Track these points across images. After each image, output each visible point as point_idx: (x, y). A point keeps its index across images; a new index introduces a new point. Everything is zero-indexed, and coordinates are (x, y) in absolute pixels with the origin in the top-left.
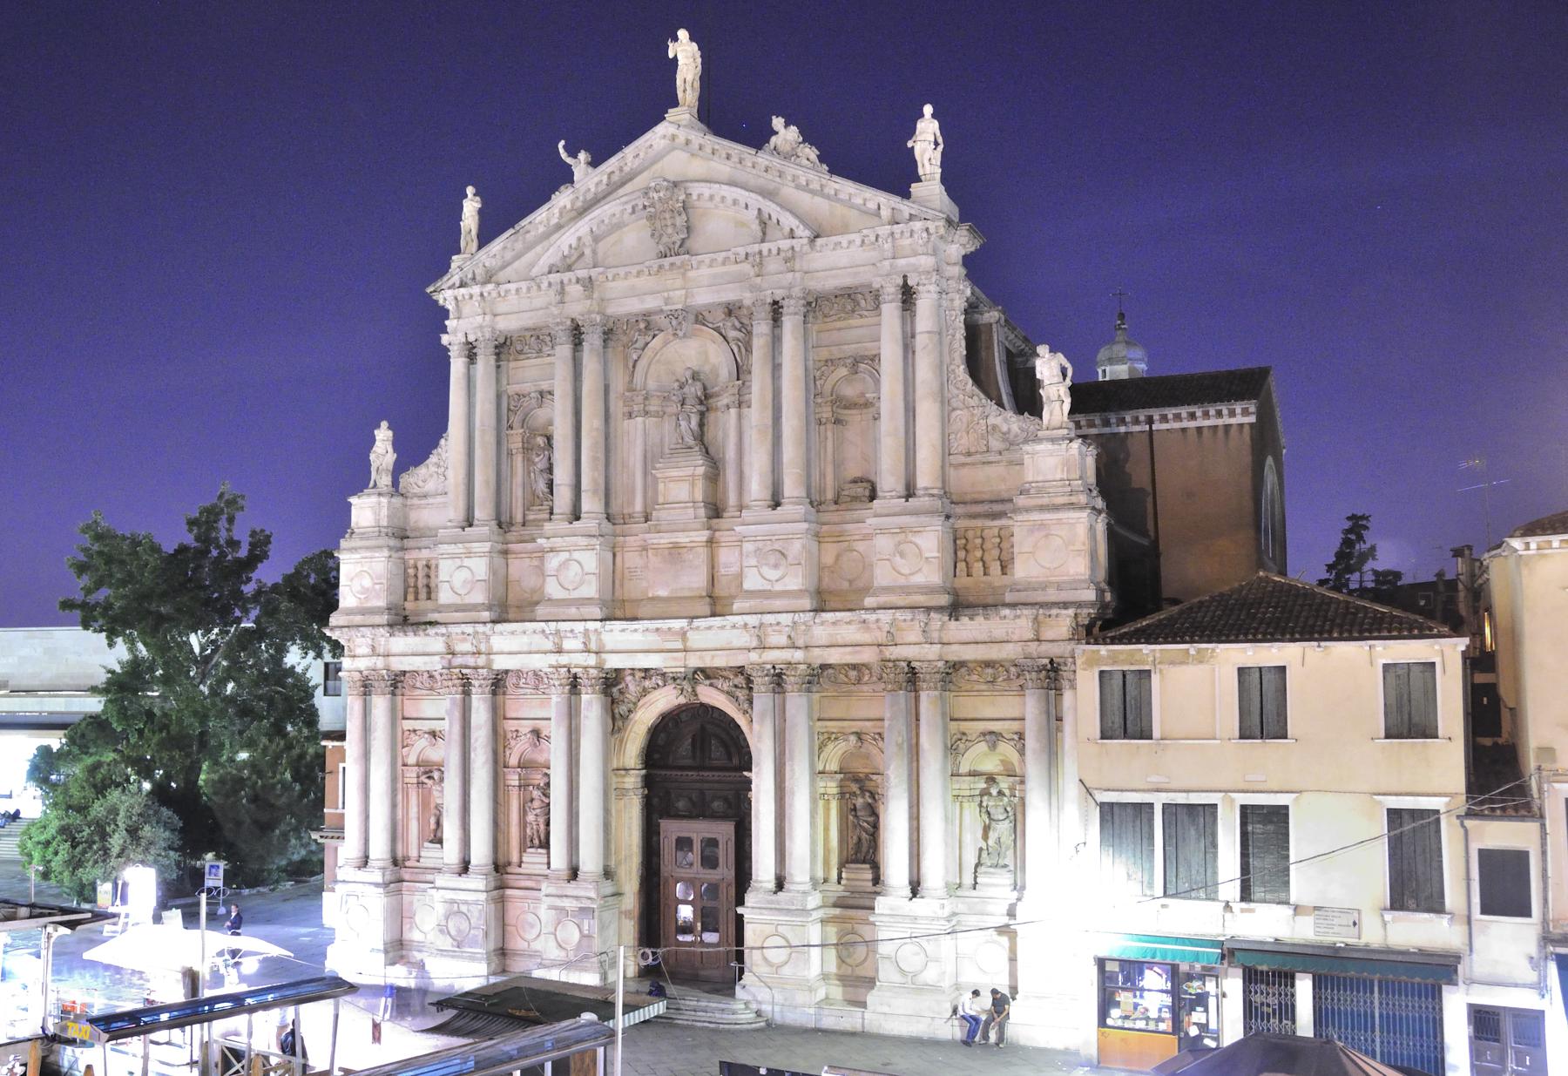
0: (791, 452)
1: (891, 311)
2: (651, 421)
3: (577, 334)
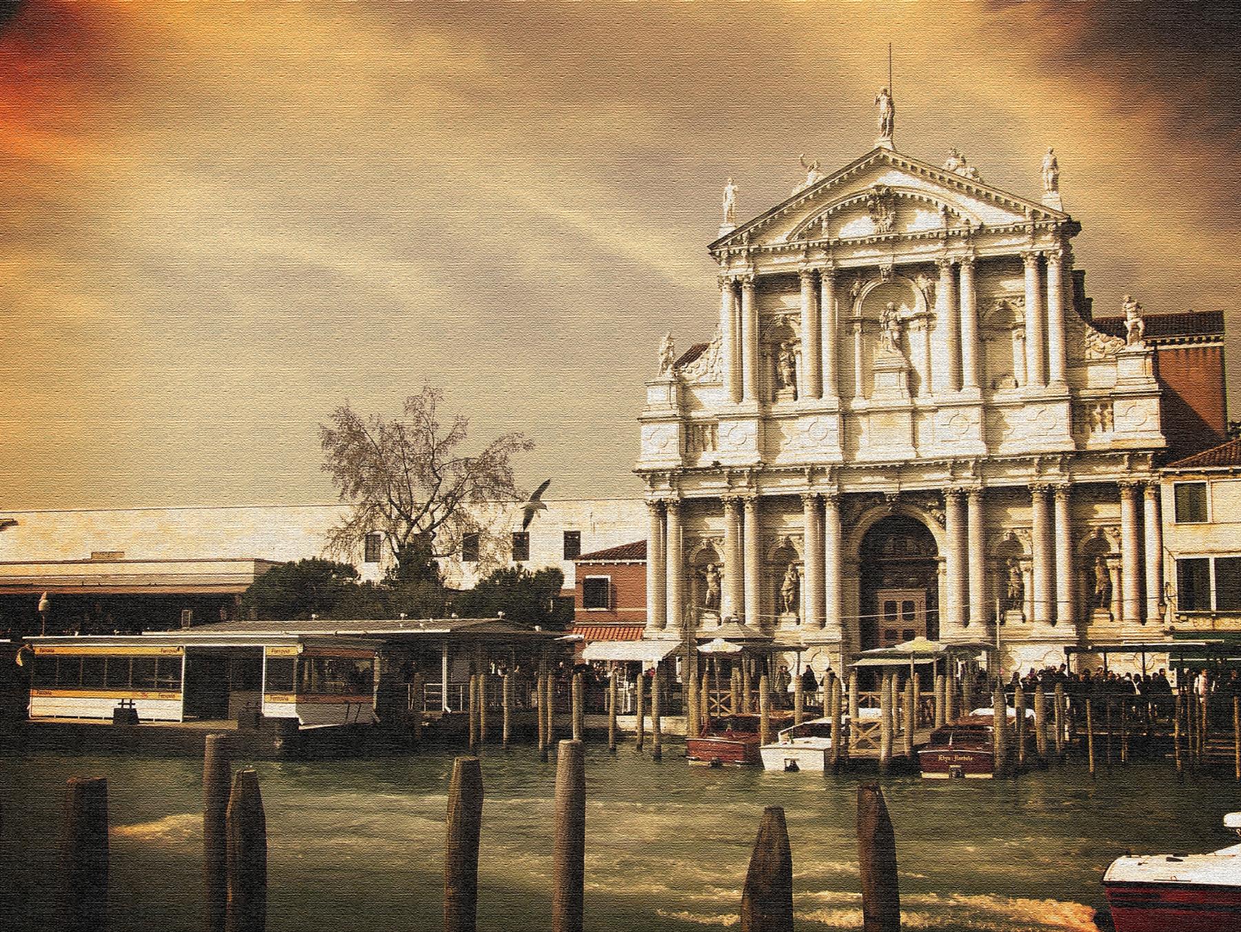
1: (1030, 271)
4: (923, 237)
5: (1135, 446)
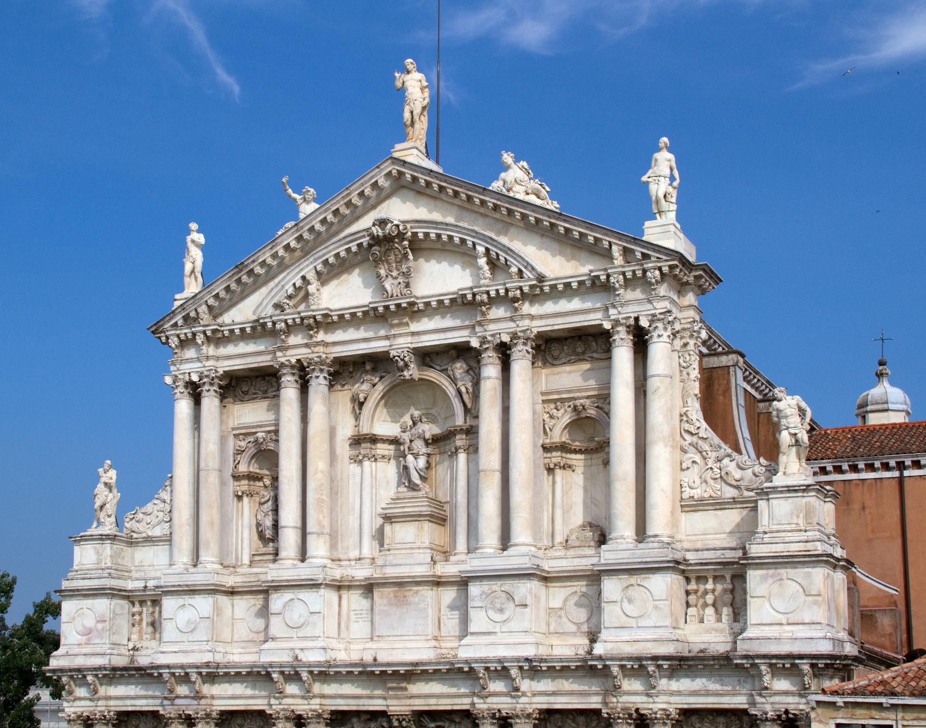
0: (520, 496)
1: (623, 354)
2: (380, 464)
3: (303, 373)
4: (453, 301)
5: (774, 649)
